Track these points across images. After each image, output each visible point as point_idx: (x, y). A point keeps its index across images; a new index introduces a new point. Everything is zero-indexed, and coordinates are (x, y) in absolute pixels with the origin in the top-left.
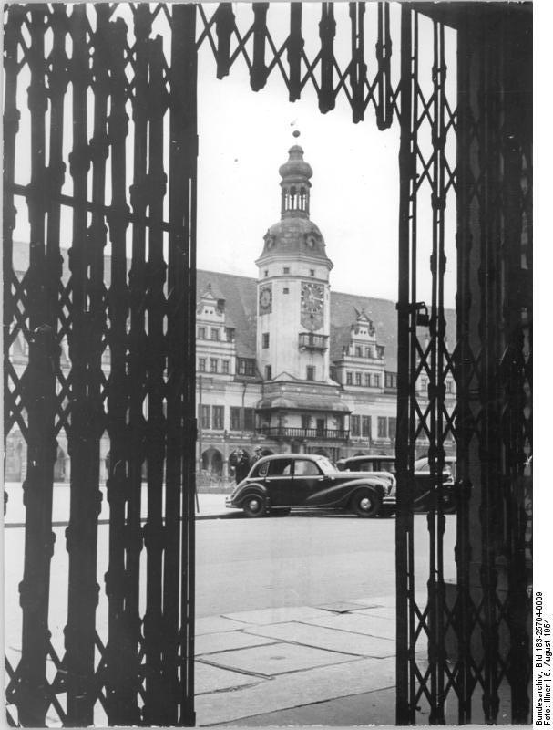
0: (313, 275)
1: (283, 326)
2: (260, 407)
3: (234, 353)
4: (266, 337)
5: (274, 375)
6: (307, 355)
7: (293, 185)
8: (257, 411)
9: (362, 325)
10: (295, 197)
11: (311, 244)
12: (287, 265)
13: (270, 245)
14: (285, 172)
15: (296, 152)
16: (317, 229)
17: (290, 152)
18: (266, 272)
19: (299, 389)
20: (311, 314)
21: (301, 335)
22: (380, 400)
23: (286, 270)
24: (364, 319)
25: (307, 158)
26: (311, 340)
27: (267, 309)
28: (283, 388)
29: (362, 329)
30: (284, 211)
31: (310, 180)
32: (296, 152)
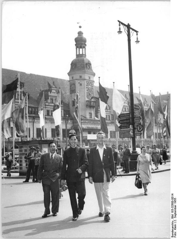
0: (90, 78)
6: (88, 109)
7: (81, 45)
11: (88, 67)
12: (81, 75)
13: (73, 67)
14: (76, 40)
15: (80, 33)
16: (90, 62)
18: (73, 77)
19: (87, 122)
21: (87, 101)
22: (110, 125)
23: (81, 77)
25: (84, 36)
30: (77, 55)
31: (86, 43)
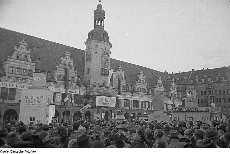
1: (95, 65)
2: (85, 95)
3: (76, 74)
4: (88, 69)
5: (91, 82)
6: (103, 76)
7: (99, 17)
8: (84, 96)
9: (120, 68)
10: (99, 22)
12: (97, 44)
17: (98, 6)
20: (105, 62)
24: (120, 66)
26: (105, 71)
27: (89, 59)
28: (95, 88)
29: (120, 69)
30: (95, 26)
32: (100, 6)
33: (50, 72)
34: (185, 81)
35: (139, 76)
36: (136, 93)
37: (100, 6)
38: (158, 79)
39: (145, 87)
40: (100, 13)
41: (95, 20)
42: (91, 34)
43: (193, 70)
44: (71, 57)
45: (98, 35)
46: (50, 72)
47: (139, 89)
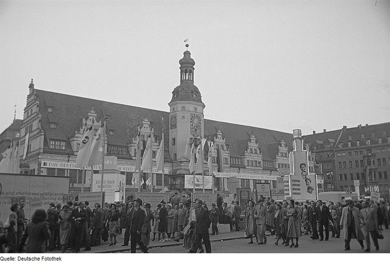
1: (182, 133)
4: (174, 139)
5: (178, 157)
8: (170, 176)
9: (219, 135)
12: (184, 105)
20: (195, 129)
24: (220, 131)
28: (182, 165)
32: (187, 54)
33: (124, 147)
34: (332, 145)
35: (249, 144)
36: (245, 168)
37: (187, 54)
38: (281, 146)
39: (259, 158)
40: (188, 63)
41: (182, 72)
42: (176, 92)
43: (345, 127)
44: (152, 124)
45: (186, 93)
46: (124, 147)
47: (250, 162)
